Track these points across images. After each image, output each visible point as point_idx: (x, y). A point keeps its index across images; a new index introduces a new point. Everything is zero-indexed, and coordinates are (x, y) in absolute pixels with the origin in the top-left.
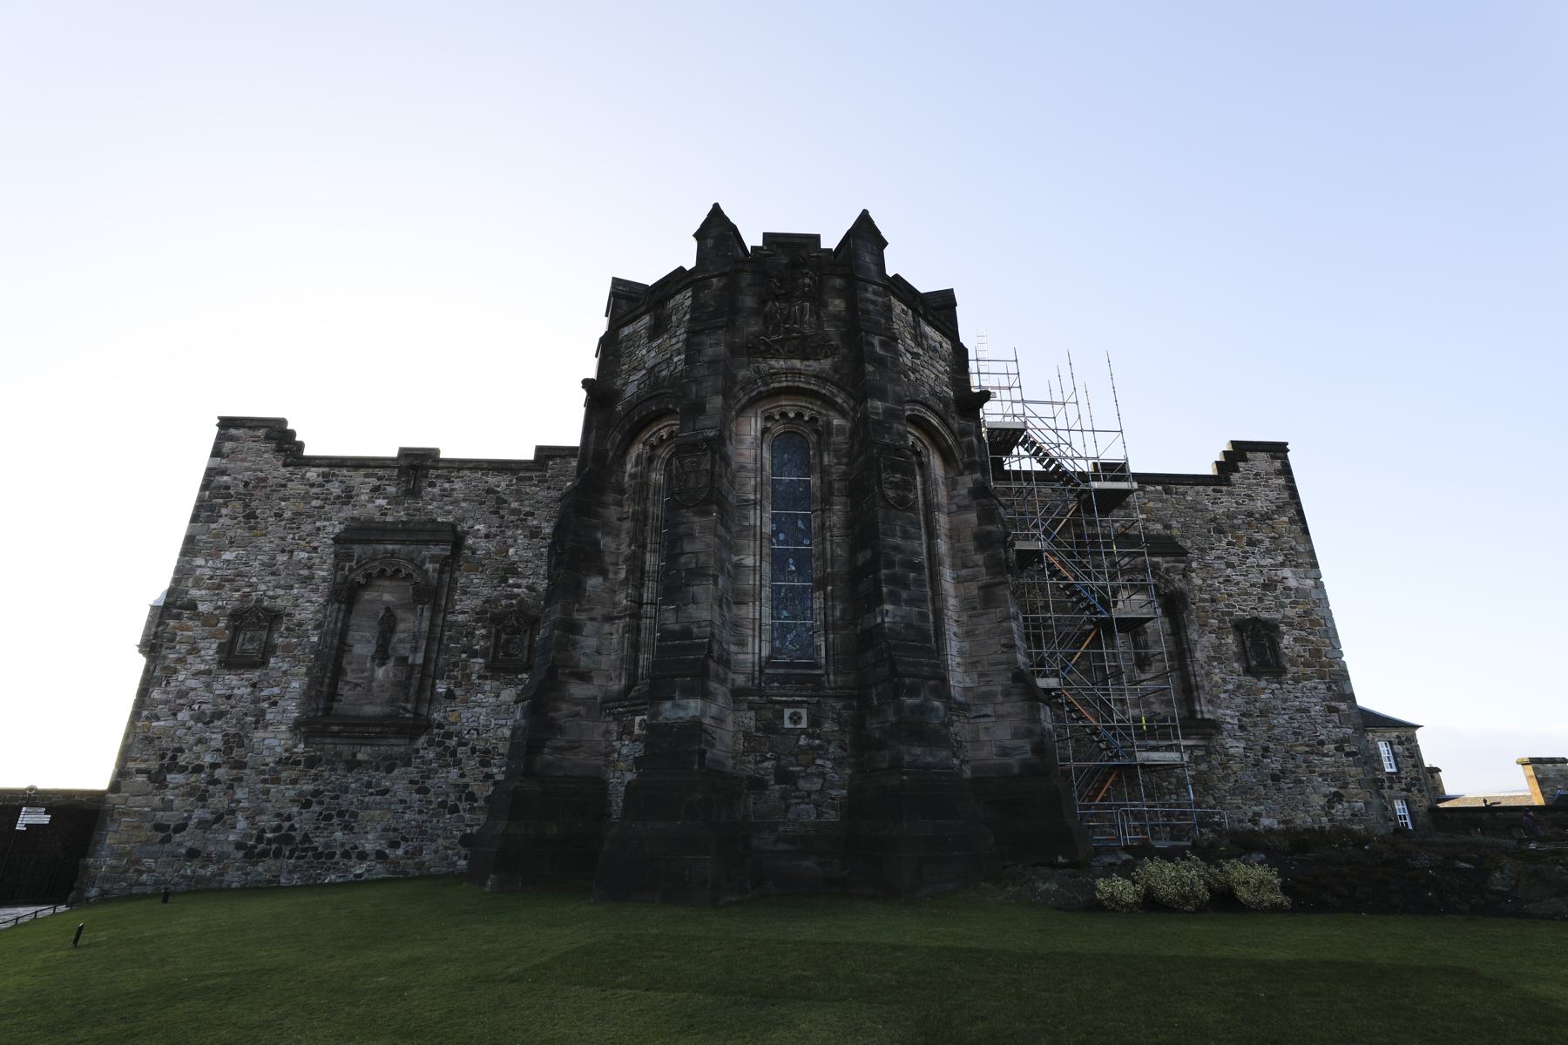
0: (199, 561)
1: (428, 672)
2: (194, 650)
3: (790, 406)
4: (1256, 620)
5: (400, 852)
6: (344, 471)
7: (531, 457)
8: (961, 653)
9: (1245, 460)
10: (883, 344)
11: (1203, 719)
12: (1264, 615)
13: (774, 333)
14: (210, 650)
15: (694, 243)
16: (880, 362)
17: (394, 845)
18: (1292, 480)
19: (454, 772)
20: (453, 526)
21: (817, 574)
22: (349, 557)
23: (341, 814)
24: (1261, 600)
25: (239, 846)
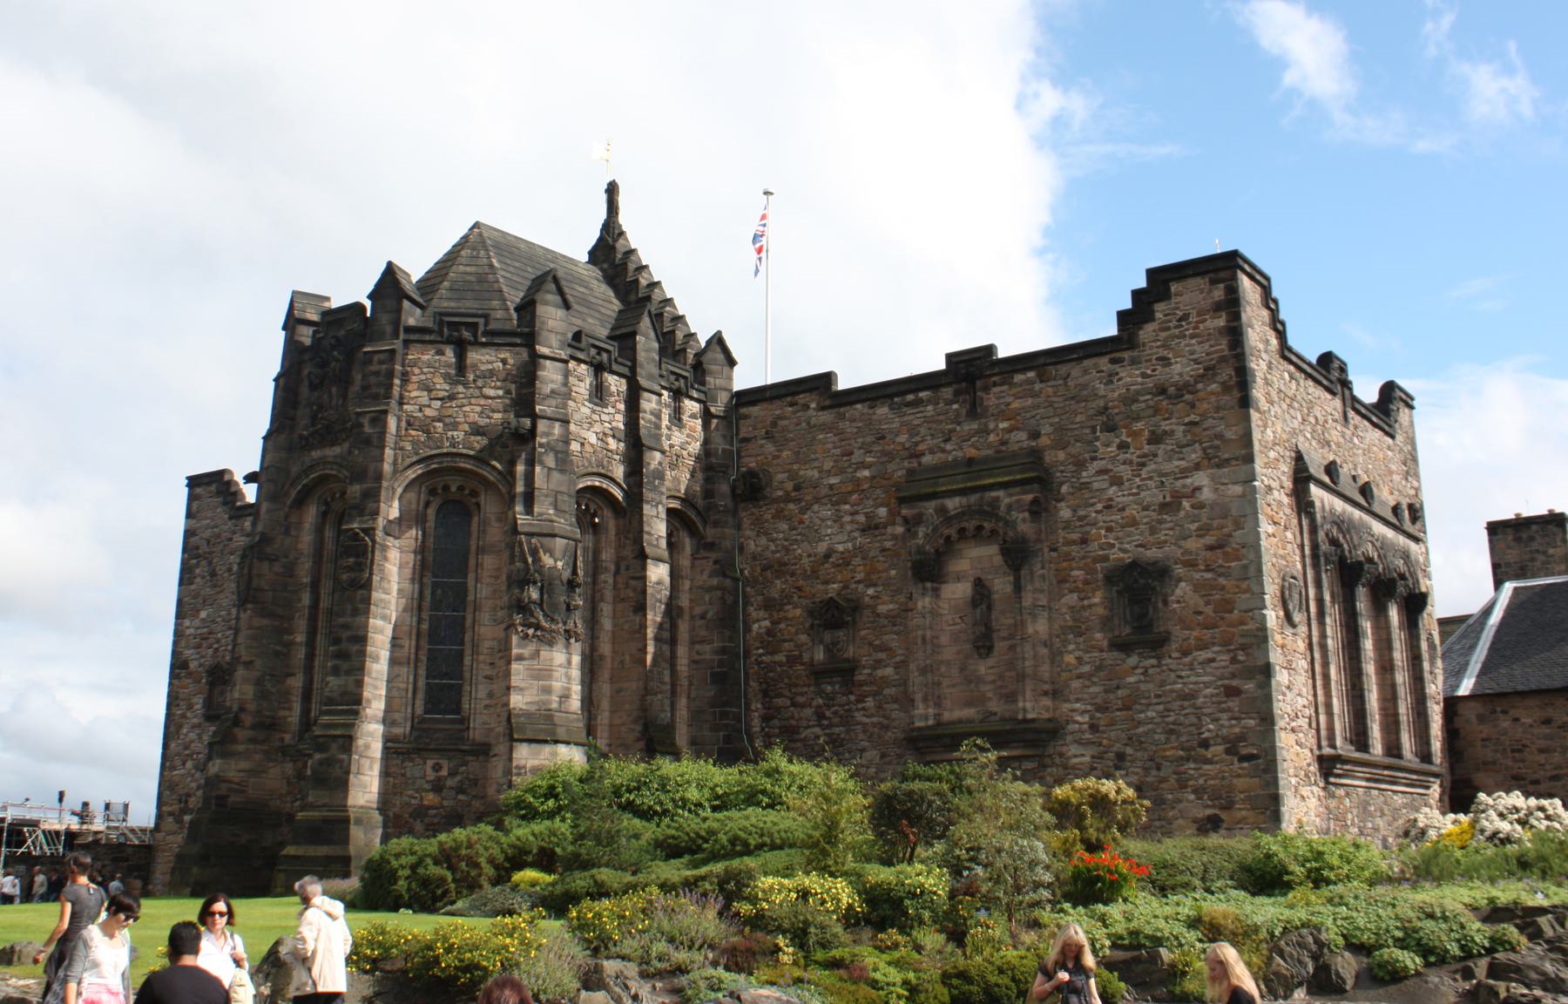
4: (1134, 564)
11: (1025, 721)
12: (1152, 554)
24: (1153, 531)
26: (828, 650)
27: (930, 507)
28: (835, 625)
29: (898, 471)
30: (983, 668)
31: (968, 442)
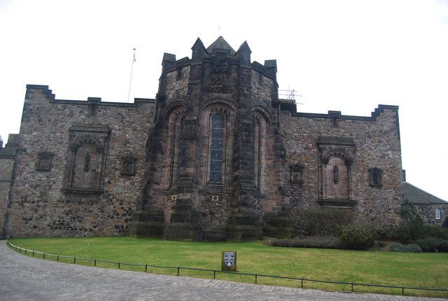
0: (26, 135)
1: (102, 175)
2: (27, 165)
3: (219, 107)
4: (376, 168)
5: (97, 229)
6: (70, 105)
7: (133, 102)
8: (265, 180)
9: (383, 111)
10: (247, 90)
12: (379, 167)
13: (215, 85)
14: (32, 165)
15: (191, 51)
16: (245, 96)
17: (95, 227)
18: (398, 120)
19: (112, 207)
20: (107, 126)
21: (224, 158)
22: (74, 136)
23: (78, 217)
25: (49, 225)
26: (295, 177)
27: (328, 147)
28: (296, 171)
29: (315, 136)
30: (335, 186)
31: (333, 133)
